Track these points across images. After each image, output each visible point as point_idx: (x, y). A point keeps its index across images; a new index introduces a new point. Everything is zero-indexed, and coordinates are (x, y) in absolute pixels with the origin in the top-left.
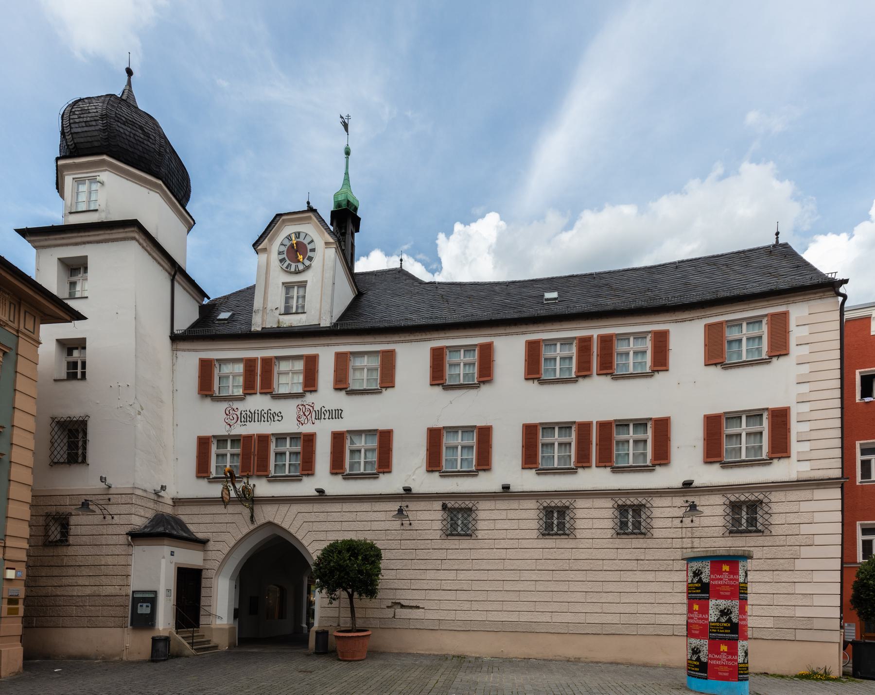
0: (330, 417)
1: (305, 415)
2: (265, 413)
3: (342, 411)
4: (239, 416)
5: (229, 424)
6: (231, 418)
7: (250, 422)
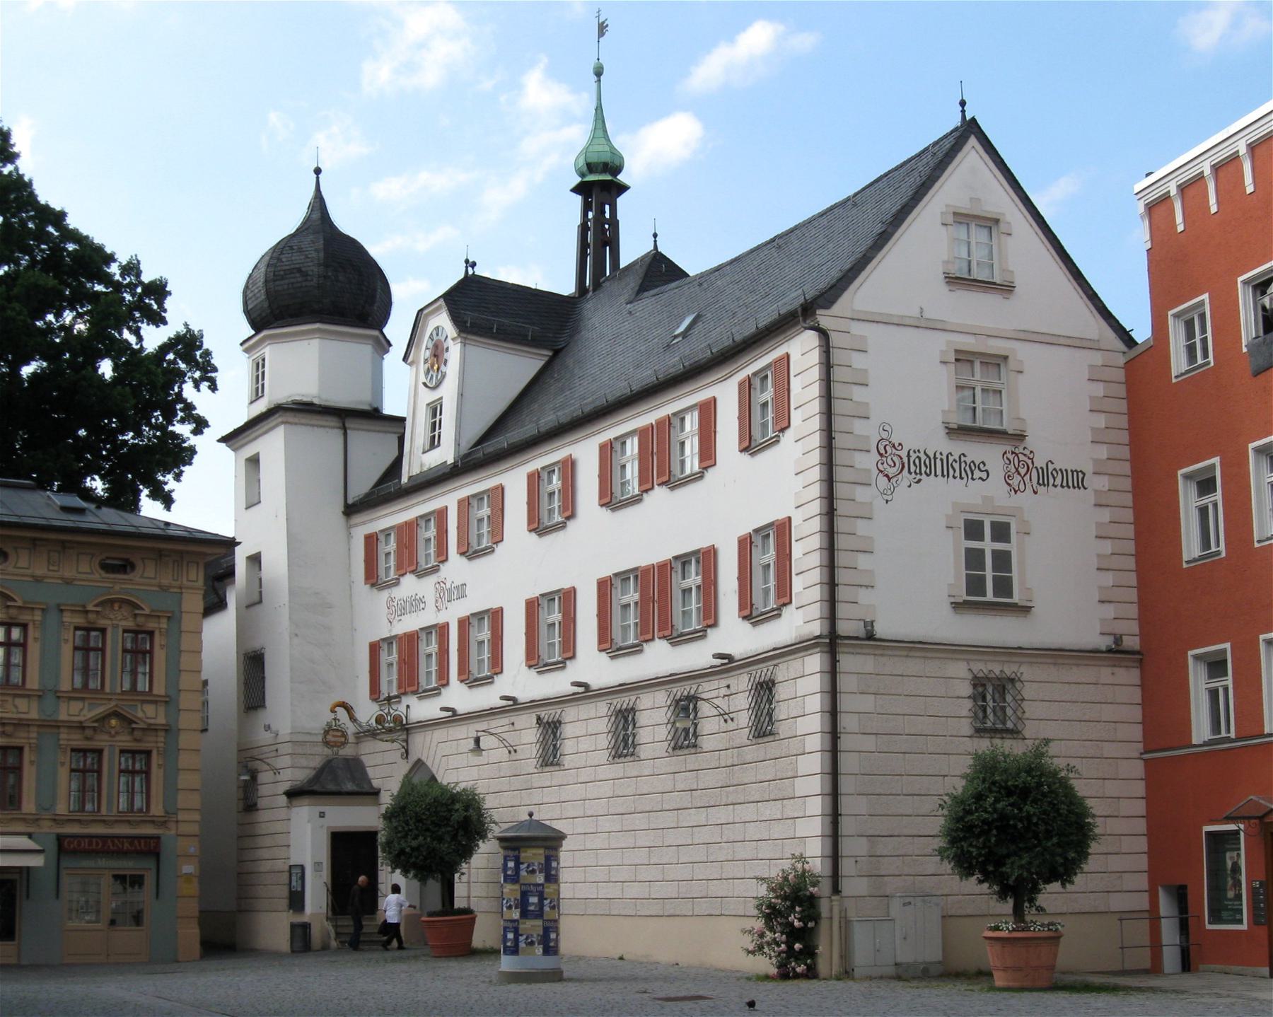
0: (1065, 484)
1: (1019, 474)
3: (1084, 474)
4: (905, 460)
5: (887, 476)
7: (928, 475)
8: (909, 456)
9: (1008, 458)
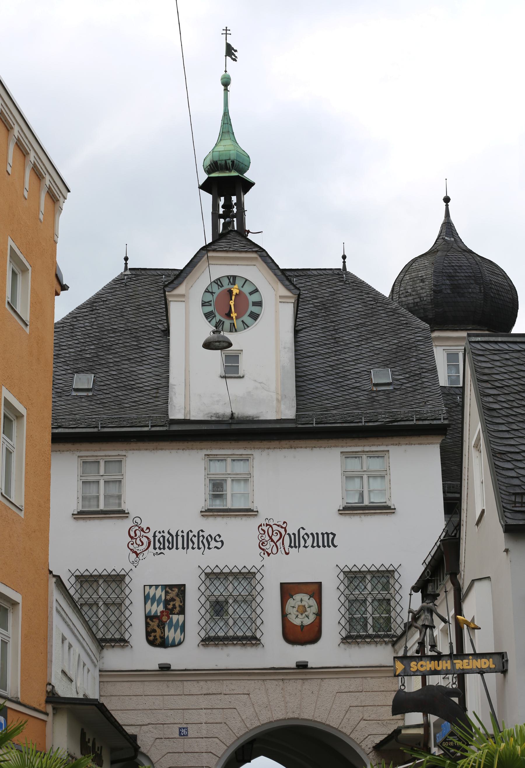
0: (315, 544)
1: (272, 541)
2: (194, 536)
3: (334, 535)
4: (152, 539)
5: (135, 552)
6: (139, 542)
8: (155, 536)
9: (262, 529)
